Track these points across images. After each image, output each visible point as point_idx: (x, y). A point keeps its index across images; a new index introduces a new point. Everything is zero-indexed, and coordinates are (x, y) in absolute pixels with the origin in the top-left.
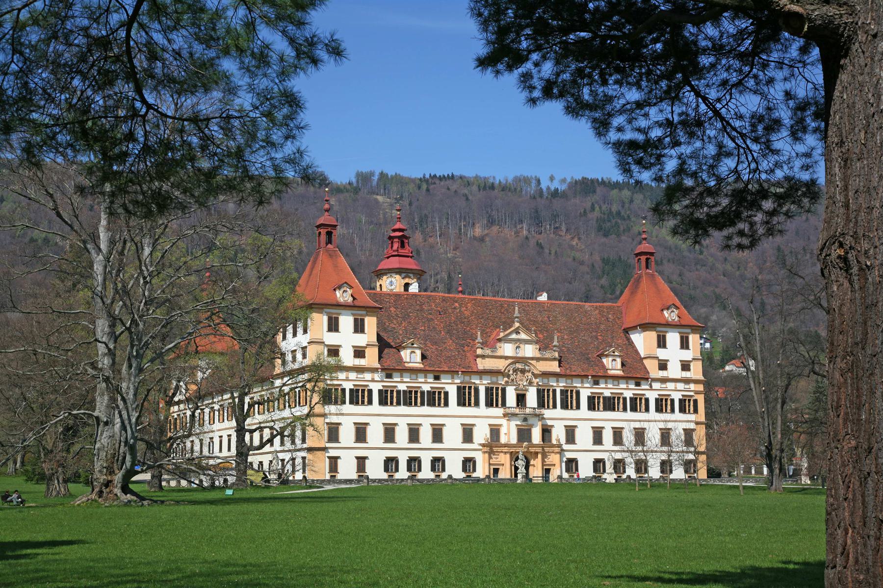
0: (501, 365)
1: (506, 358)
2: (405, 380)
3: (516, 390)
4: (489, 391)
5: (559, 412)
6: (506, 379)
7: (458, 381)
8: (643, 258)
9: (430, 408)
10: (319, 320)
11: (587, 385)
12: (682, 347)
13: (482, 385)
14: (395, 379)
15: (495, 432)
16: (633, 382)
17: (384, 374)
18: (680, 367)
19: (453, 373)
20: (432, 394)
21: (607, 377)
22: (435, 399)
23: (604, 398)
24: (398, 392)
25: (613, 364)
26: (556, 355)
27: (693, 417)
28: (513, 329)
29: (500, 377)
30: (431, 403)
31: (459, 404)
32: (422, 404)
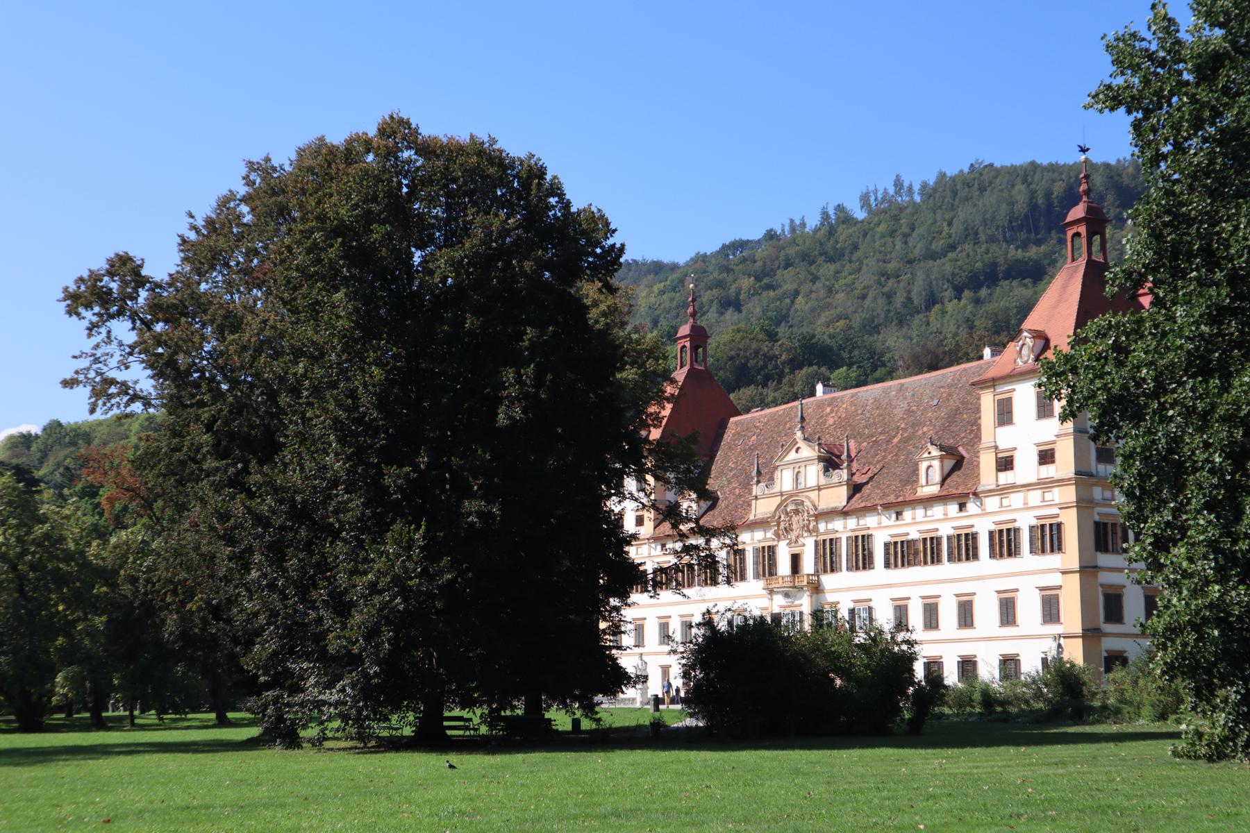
18: (1036, 458)
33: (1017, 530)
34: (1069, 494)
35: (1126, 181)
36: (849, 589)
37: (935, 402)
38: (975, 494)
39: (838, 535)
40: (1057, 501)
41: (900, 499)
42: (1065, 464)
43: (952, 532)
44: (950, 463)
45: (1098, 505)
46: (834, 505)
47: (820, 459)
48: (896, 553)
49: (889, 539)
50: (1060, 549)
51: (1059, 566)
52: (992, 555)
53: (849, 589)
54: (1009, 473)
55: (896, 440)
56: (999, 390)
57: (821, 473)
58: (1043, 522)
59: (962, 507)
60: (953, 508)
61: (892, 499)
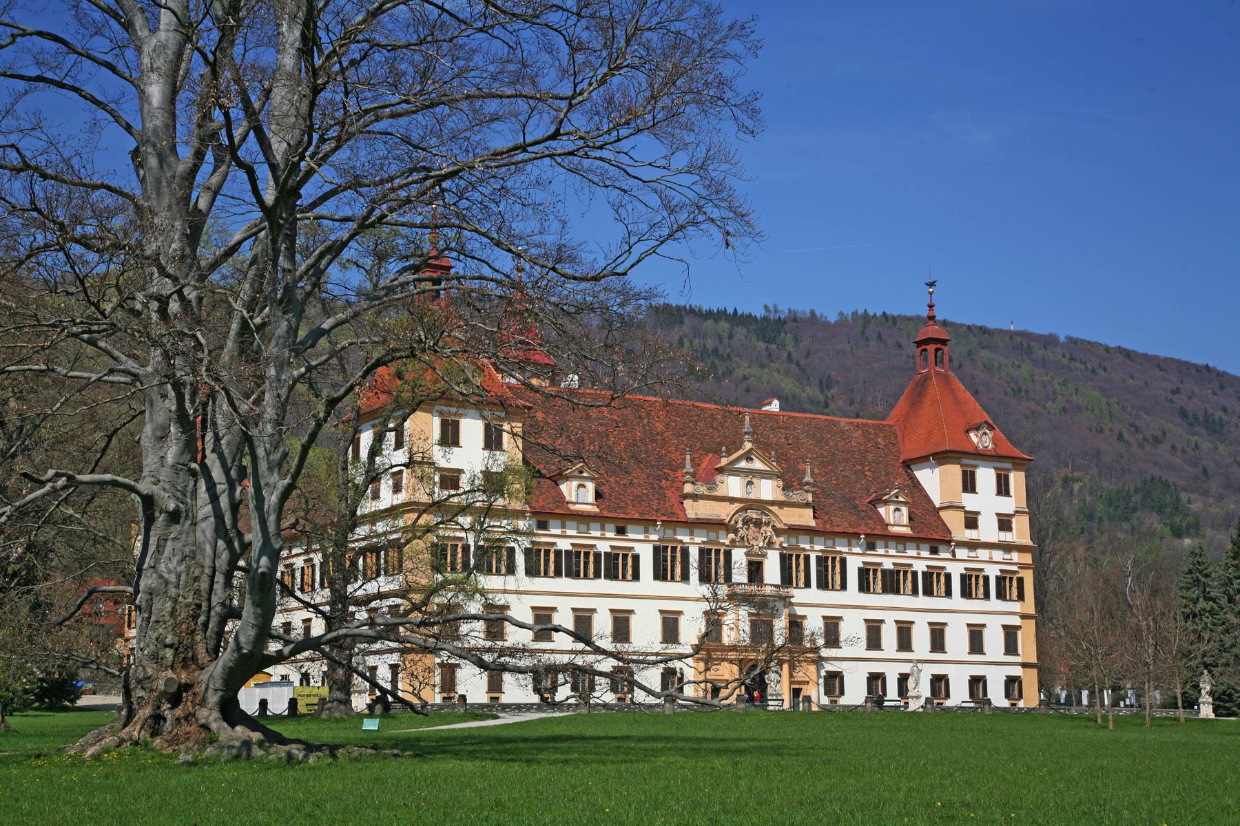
0: (724, 511)
1: (732, 500)
2: (569, 532)
3: (747, 554)
4: (704, 553)
5: (813, 594)
6: (732, 536)
7: (654, 537)
8: (931, 348)
9: (608, 582)
10: (424, 426)
11: (857, 550)
12: (999, 493)
13: (694, 543)
14: (553, 531)
15: (714, 622)
16: (927, 546)
17: (533, 522)
19: (647, 523)
20: (611, 558)
21: (889, 538)
22: (616, 566)
23: (884, 572)
24: (558, 553)
25: (895, 517)
26: (810, 498)
27: (1016, 607)
28: (741, 452)
29: (722, 533)
30: (612, 575)
31: (656, 577)
32: (597, 575)
51: (1018, 610)
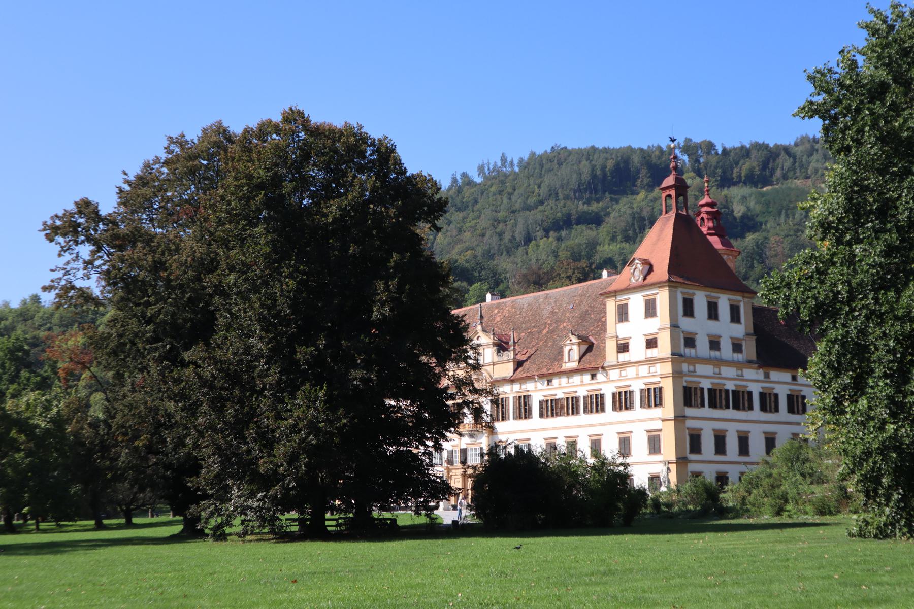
18: (644, 344)
27: (656, 412)
33: (631, 392)
34: (668, 368)
35: (654, 160)
36: (514, 432)
37: (571, 306)
38: (603, 368)
39: (507, 396)
40: (659, 373)
41: (551, 371)
42: (664, 348)
43: (586, 393)
44: (584, 347)
45: (685, 375)
46: (504, 375)
47: (494, 344)
48: (547, 407)
49: (542, 398)
50: (661, 404)
52: (615, 409)
53: (514, 432)
54: (626, 354)
55: (544, 332)
56: (619, 298)
57: (495, 354)
58: (649, 387)
59: (593, 376)
60: (587, 377)
61: (545, 371)
